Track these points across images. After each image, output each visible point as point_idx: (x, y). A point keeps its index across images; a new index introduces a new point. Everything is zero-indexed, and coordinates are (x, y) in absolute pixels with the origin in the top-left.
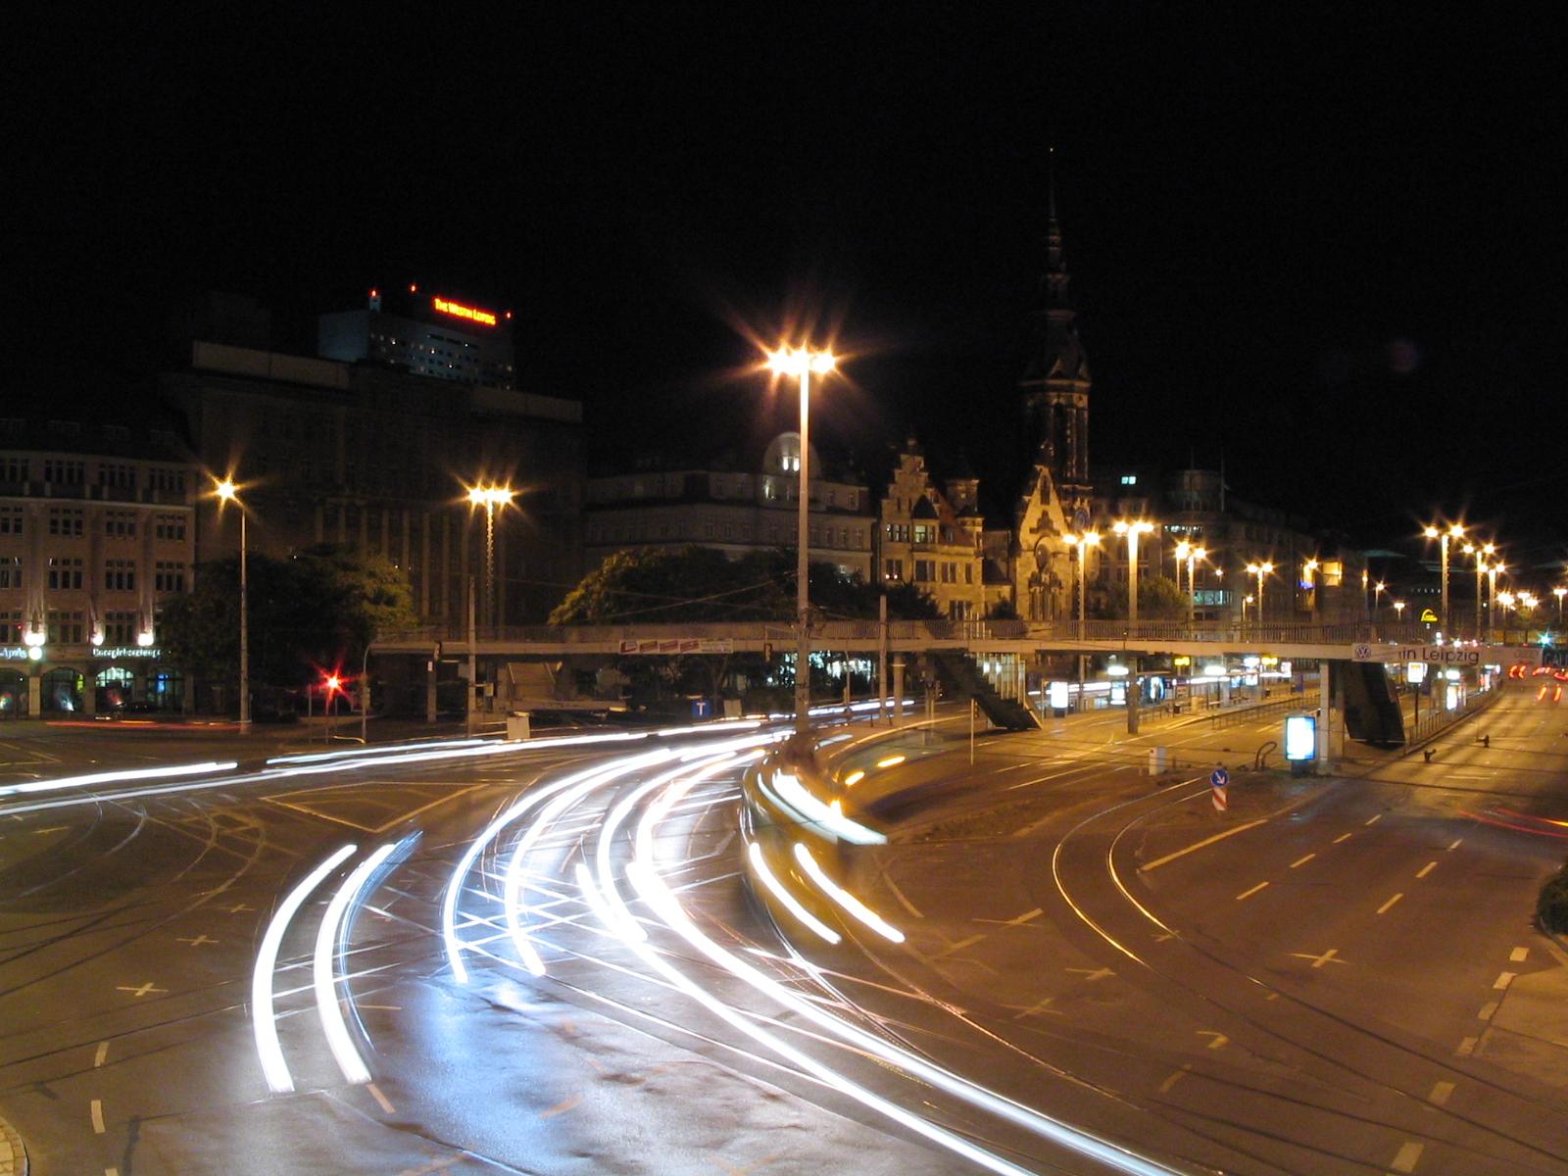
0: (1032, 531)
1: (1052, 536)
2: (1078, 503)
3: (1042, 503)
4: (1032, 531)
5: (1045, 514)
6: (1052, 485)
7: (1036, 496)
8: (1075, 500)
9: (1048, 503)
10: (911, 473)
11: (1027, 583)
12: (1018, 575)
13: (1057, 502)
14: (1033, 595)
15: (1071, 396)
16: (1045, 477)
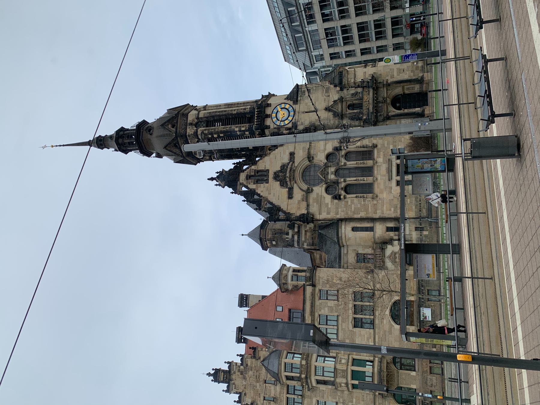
0: (290, 196)
1: (296, 164)
2: (268, 122)
3: (267, 181)
4: (290, 196)
5: (276, 177)
6: (253, 167)
7: (261, 189)
8: (268, 127)
9: (268, 171)
10: (245, 378)
11: (336, 201)
12: (329, 217)
13: (266, 159)
14: (348, 189)
15: (189, 136)
16: (248, 177)
